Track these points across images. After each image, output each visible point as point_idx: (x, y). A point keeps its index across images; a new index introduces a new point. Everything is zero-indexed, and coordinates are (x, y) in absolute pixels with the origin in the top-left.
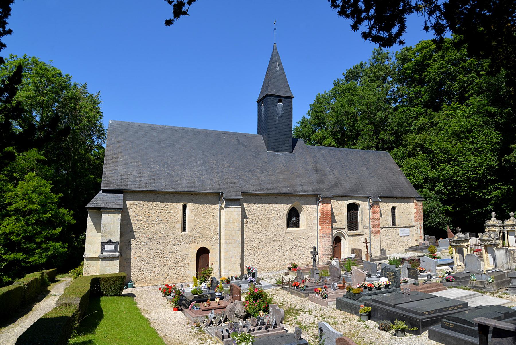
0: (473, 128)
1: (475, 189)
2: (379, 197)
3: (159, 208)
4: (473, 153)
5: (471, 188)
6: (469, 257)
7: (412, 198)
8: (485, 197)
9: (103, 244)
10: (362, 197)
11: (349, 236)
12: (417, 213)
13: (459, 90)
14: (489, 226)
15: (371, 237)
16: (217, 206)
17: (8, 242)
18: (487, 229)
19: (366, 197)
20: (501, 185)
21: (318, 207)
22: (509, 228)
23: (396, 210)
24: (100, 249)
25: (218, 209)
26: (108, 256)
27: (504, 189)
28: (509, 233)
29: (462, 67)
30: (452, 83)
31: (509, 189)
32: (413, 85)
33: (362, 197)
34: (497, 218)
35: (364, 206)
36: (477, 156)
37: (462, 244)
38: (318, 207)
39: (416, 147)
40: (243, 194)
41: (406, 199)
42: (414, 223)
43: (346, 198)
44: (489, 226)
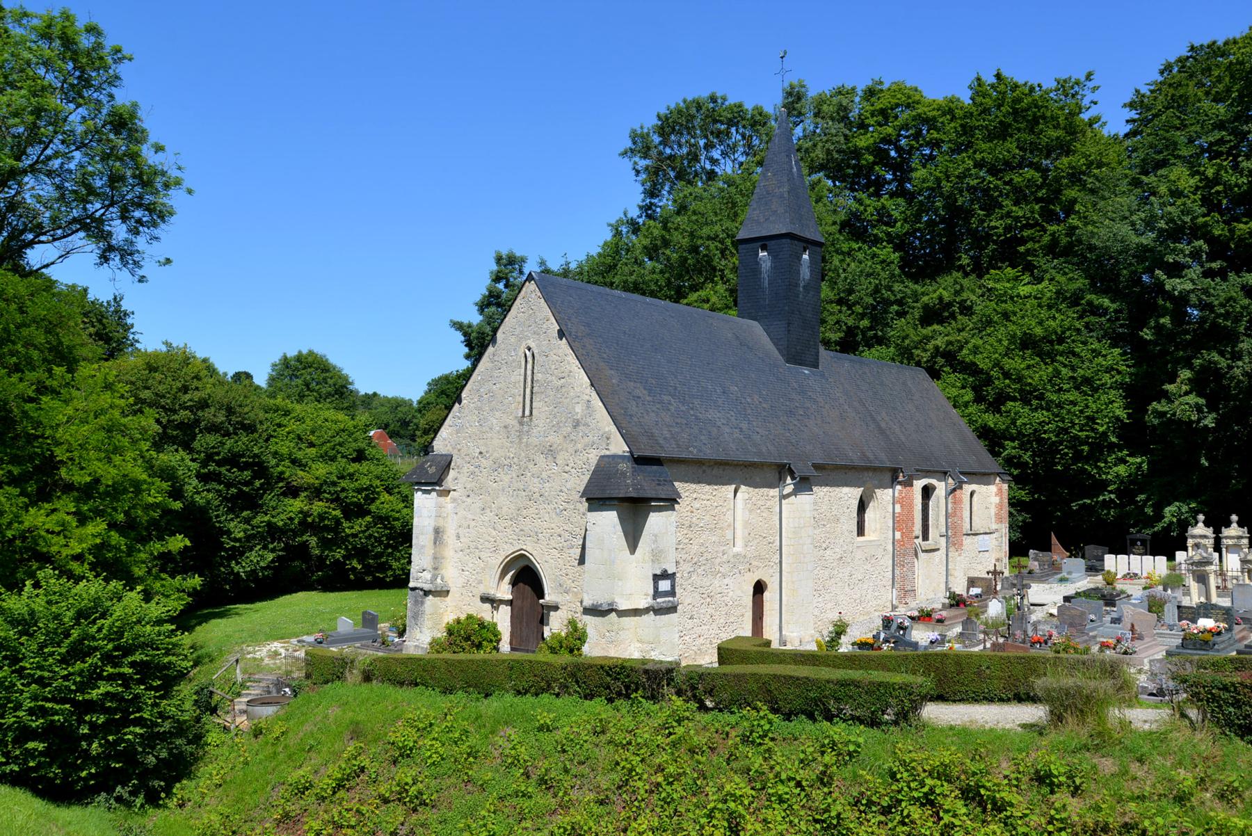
0: (1068, 333)
1: (1087, 459)
2: (962, 473)
3: (703, 497)
4: (1077, 388)
5: (1078, 456)
6: (1240, 589)
7: (992, 474)
8: (1100, 476)
9: (656, 578)
10: (937, 472)
11: (923, 551)
12: (1000, 506)
13: (1005, 235)
14: (1193, 537)
15: (950, 555)
16: (774, 492)
17: (352, 576)
18: (1190, 542)
19: (941, 472)
20: (1127, 455)
21: (894, 493)
22: (1230, 542)
23: (975, 496)
24: (651, 592)
25: (778, 499)
26: (664, 605)
27: (1132, 464)
28: (1230, 549)
29: (1009, 183)
30: (988, 216)
31: (1139, 467)
32: (871, 190)
33: (937, 472)
34: (1207, 524)
35: (941, 488)
36: (1086, 394)
37: (1207, 568)
38: (894, 493)
39: (936, 357)
40: (817, 467)
41: (982, 477)
42: (994, 526)
43: (924, 474)
44: (1193, 537)
